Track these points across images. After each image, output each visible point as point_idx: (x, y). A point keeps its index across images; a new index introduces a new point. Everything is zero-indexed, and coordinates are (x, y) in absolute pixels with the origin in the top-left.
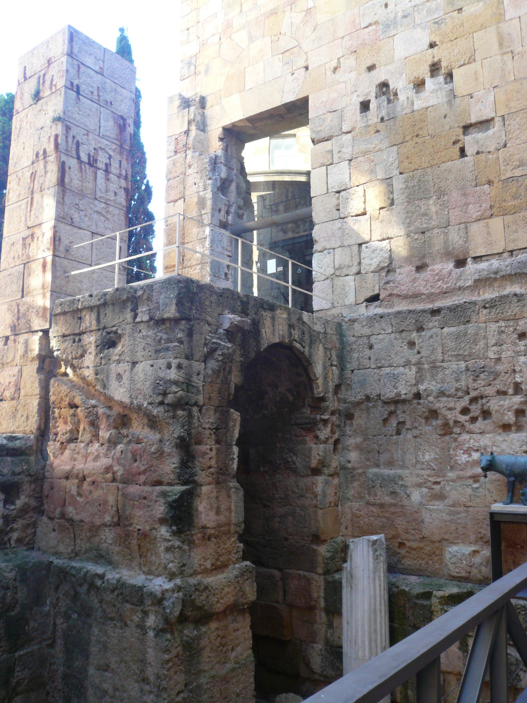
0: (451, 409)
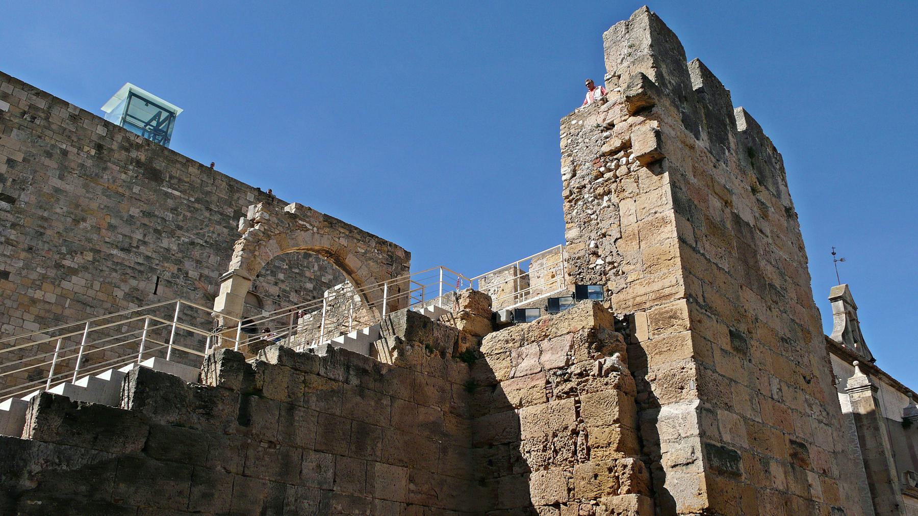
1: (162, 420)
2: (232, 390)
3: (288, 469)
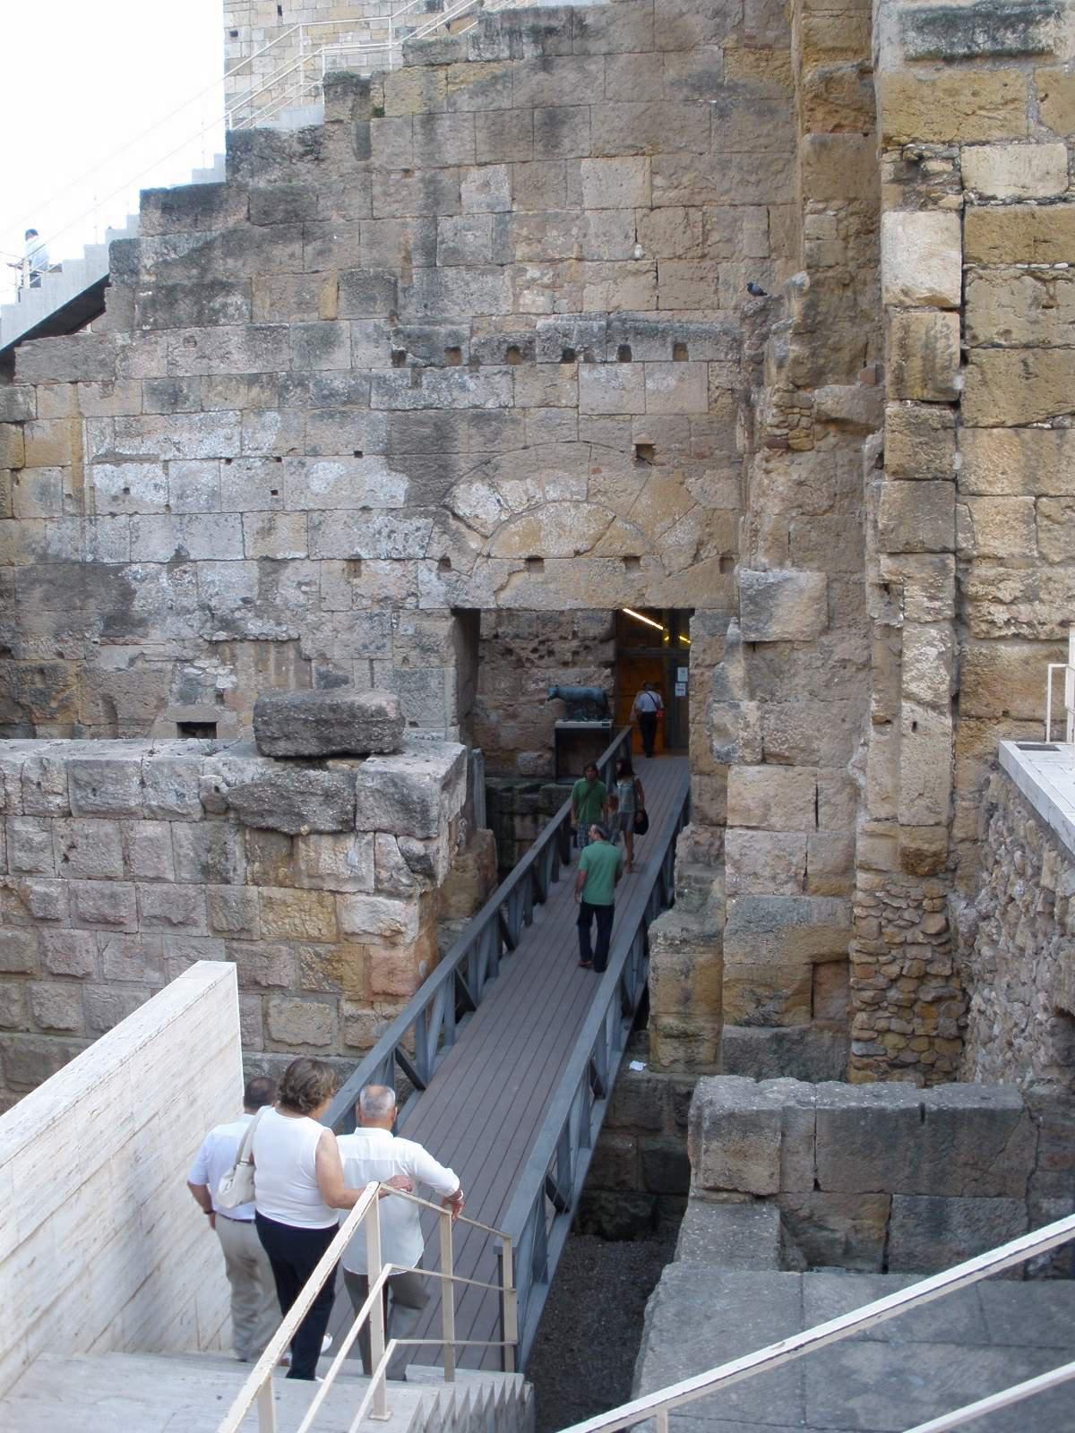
0: (524, 649)
1: (261, 183)
2: (341, 122)
3: (437, 199)
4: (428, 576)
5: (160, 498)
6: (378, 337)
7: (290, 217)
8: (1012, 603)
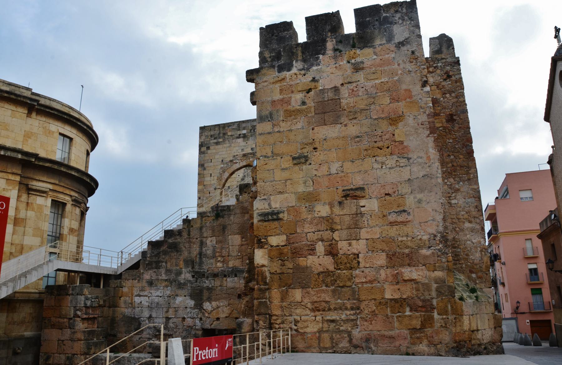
1: (170, 241)
3: (202, 244)
4: (197, 321)
5: (147, 304)
6: (189, 272)
7: (175, 247)
8: (280, 324)
